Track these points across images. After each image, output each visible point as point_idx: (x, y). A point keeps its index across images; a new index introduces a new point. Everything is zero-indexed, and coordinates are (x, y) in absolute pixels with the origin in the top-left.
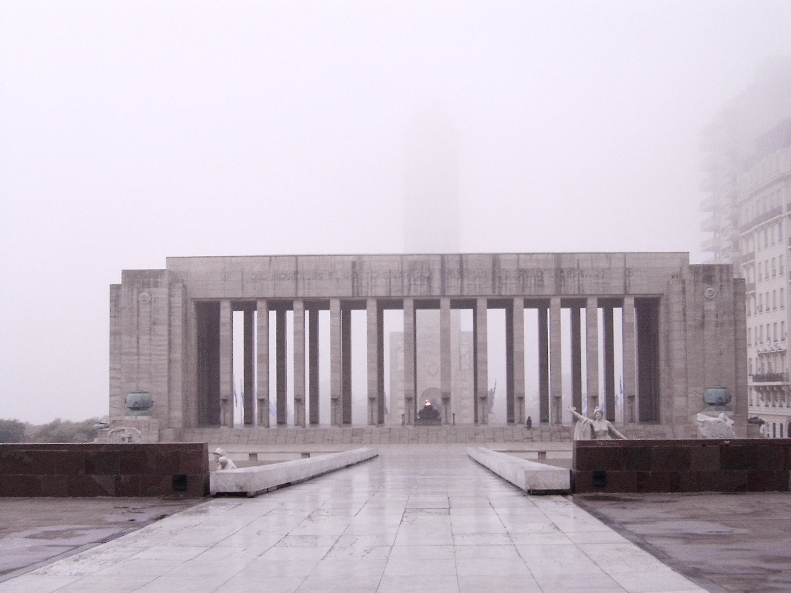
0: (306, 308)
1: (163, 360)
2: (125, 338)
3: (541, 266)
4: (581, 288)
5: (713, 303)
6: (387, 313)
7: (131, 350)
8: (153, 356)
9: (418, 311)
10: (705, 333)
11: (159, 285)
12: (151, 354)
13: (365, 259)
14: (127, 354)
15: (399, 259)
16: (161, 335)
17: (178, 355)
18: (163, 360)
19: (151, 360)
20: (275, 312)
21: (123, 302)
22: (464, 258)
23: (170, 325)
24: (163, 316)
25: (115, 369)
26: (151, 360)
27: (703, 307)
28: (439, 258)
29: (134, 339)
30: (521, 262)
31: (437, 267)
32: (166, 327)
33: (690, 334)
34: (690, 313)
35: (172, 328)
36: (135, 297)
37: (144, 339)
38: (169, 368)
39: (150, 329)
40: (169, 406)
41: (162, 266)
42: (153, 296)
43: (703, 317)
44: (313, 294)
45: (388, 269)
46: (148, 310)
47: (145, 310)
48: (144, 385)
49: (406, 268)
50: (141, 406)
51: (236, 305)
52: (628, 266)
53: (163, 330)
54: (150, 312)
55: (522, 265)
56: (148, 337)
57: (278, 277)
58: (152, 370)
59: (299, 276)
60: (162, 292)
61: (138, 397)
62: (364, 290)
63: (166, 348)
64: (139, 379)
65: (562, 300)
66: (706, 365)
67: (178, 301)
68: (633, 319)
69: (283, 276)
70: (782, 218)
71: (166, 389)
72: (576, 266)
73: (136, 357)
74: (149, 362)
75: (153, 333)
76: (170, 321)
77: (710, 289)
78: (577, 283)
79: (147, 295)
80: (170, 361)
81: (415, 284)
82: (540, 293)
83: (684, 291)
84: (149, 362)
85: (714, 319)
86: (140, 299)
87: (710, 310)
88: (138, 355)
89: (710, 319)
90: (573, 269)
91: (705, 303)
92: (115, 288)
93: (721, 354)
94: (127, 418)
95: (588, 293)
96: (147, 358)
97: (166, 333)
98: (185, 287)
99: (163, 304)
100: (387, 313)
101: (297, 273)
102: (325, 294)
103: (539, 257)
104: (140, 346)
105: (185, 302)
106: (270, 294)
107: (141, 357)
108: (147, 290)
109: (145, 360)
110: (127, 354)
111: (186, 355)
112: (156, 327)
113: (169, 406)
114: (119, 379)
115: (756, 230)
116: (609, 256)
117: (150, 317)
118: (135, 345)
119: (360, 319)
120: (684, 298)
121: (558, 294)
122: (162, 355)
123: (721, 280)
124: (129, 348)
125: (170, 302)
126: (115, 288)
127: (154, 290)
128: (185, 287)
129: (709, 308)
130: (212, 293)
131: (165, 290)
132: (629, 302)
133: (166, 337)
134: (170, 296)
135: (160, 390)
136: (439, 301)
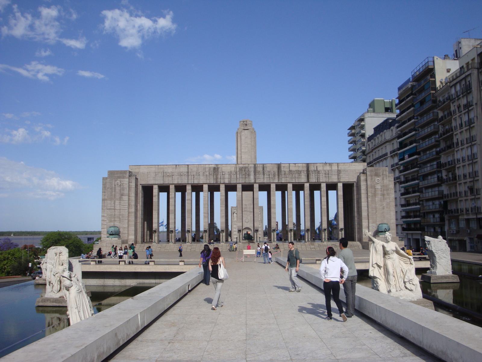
0: (193, 191)
1: (126, 212)
2: (109, 202)
3: (300, 169)
4: (318, 179)
5: (378, 185)
6: (230, 193)
7: (111, 207)
8: (121, 210)
9: (243, 192)
10: (376, 199)
11: (125, 177)
12: (120, 210)
13: (219, 166)
14: (110, 209)
15: (235, 166)
16: (125, 201)
17: (133, 210)
18: (126, 212)
19: (120, 212)
20: (180, 193)
21: (108, 185)
22: (265, 166)
23: (129, 196)
24: (126, 192)
25: (104, 216)
26: (120, 212)
27: (375, 187)
28: (253, 166)
29: (113, 202)
30: (290, 167)
31: (252, 170)
32: (127, 197)
33: (369, 199)
34: (369, 190)
35: (130, 198)
36: (113, 183)
37: (117, 202)
38: (128, 216)
39: (120, 198)
40: (128, 233)
41: (127, 168)
42: (122, 183)
43: (375, 191)
44: (196, 182)
45: (230, 170)
46: (119, 189)
47: (118, 189)
48: (117, 224)
49: (238, 170)
50: (114, 233)
51: (164, 188)
52: (339, 169)
53: (126, 198)
54: (120, 190)
55: (291, 168)
56: (119, 201)
57: (180, 175)
58: (121, 217)
59: (189, 174)
60: (126, 181)
61: (112, 229)
62: (219, 180)
63: (127, 206)
64: (115, 221)
65: (310, 184)
66: (377, 214)
67: (133, 184)
68: (341, 193)
69: (182, 174)
70: (388, 157)
71: (127, 226)
72: (316, 169)
73: (113, 211)
74: (119, 213)
75: (121, 200)
76: (129, 194)
77: (378, 178)
78: (316, 177)
79: (119, 182)
80: (129, 213)
81: (242, 178)
82: (300, 181)
83: (366, 180)
84: (119, 213)
85: (380, 192)
86: (116, 184)
87: (378, 188)
88: (115, 209)
89: (379, 192)
90: (315, 171)
91: (376, 185)
92: (104, 179)
93: (384, 209)
94: (108, 239)
95: (322, 181)
96: (119, 211)
97: (127, 199)
98: (137, 179)
99: (126, 186)
100: (230, 193)
101: (188, 172)
102: (201, 182)
103: (299, 165)
104: (116, 206)
105: (136, 186)
106: (176, 182)
107: (116, 211)
108: (119, 180)
109: (118, 212)
110: (110, 209)
111: (136, 210)
112: (123, 197)
113: (128, 233)
114: (106, 221)
115: (375, 163)
116: (330, 164)
117: (120, 192)
118: (113, 205)
119: (218, 196)
120: (367, 183)
121: (308, 182)
122: (125, 210)
123: (383, 174)
124: (111, 206)
125: (129, 185)
126: (104, 179)
127: (122, 179)
128: (137, 179)
129: (378, 187)
130: (150, 181)
131: (127, 180)
132: (340, 186)
133: (127, 202)
134: (129, 183)
135: (124, 226)
136: (253, 186)
